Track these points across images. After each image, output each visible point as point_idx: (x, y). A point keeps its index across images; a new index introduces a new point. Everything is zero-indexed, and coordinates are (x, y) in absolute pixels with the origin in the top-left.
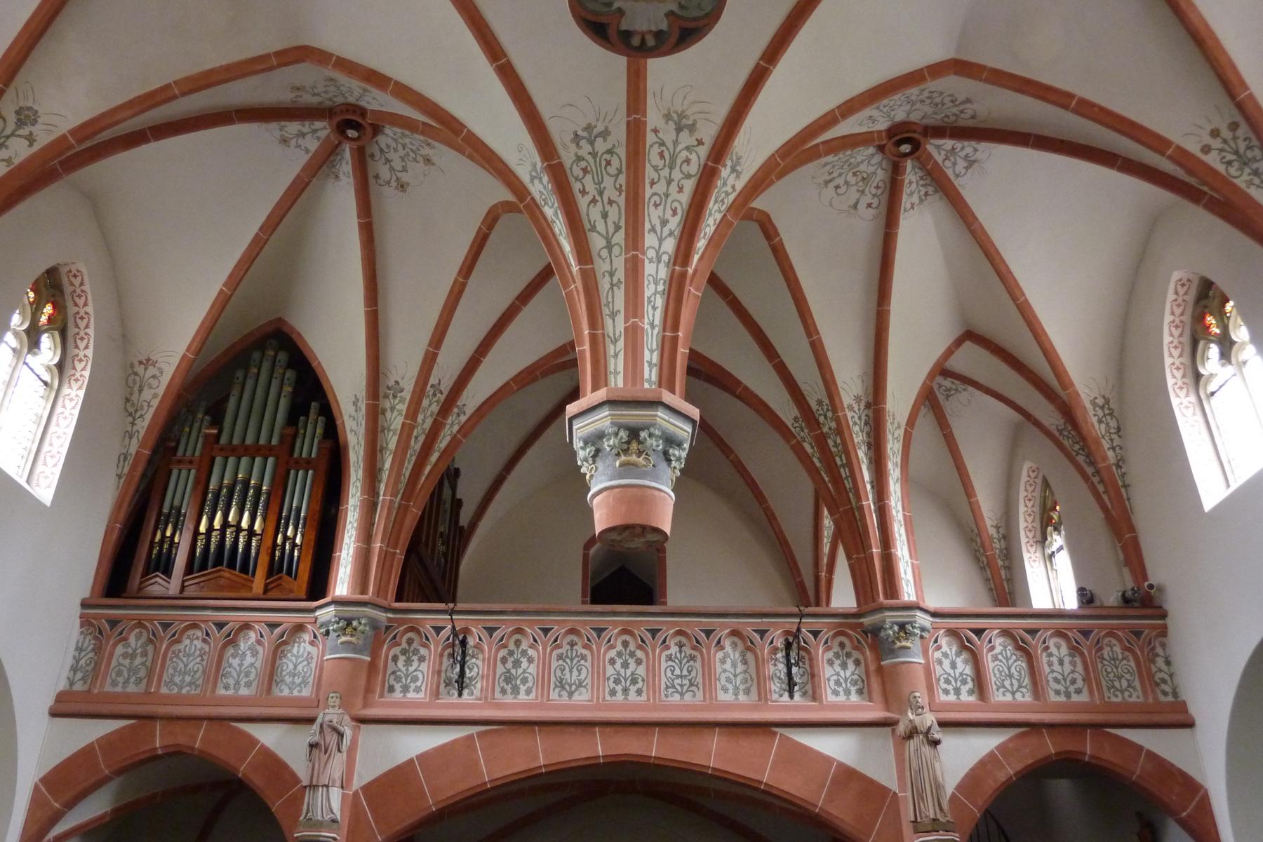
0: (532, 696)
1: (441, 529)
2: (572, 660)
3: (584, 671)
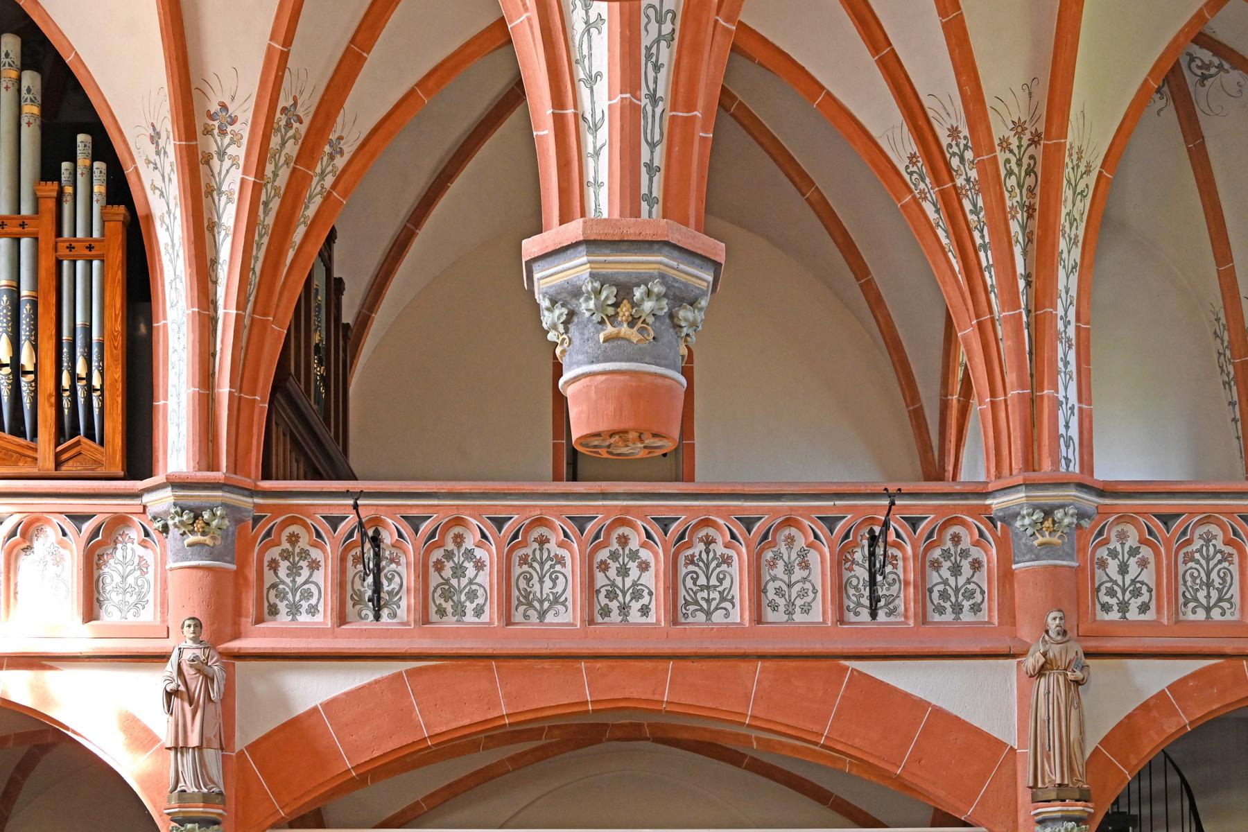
0: (485, 618)
1: (316, 338)
2: (542, 564)
3: (561, 580)
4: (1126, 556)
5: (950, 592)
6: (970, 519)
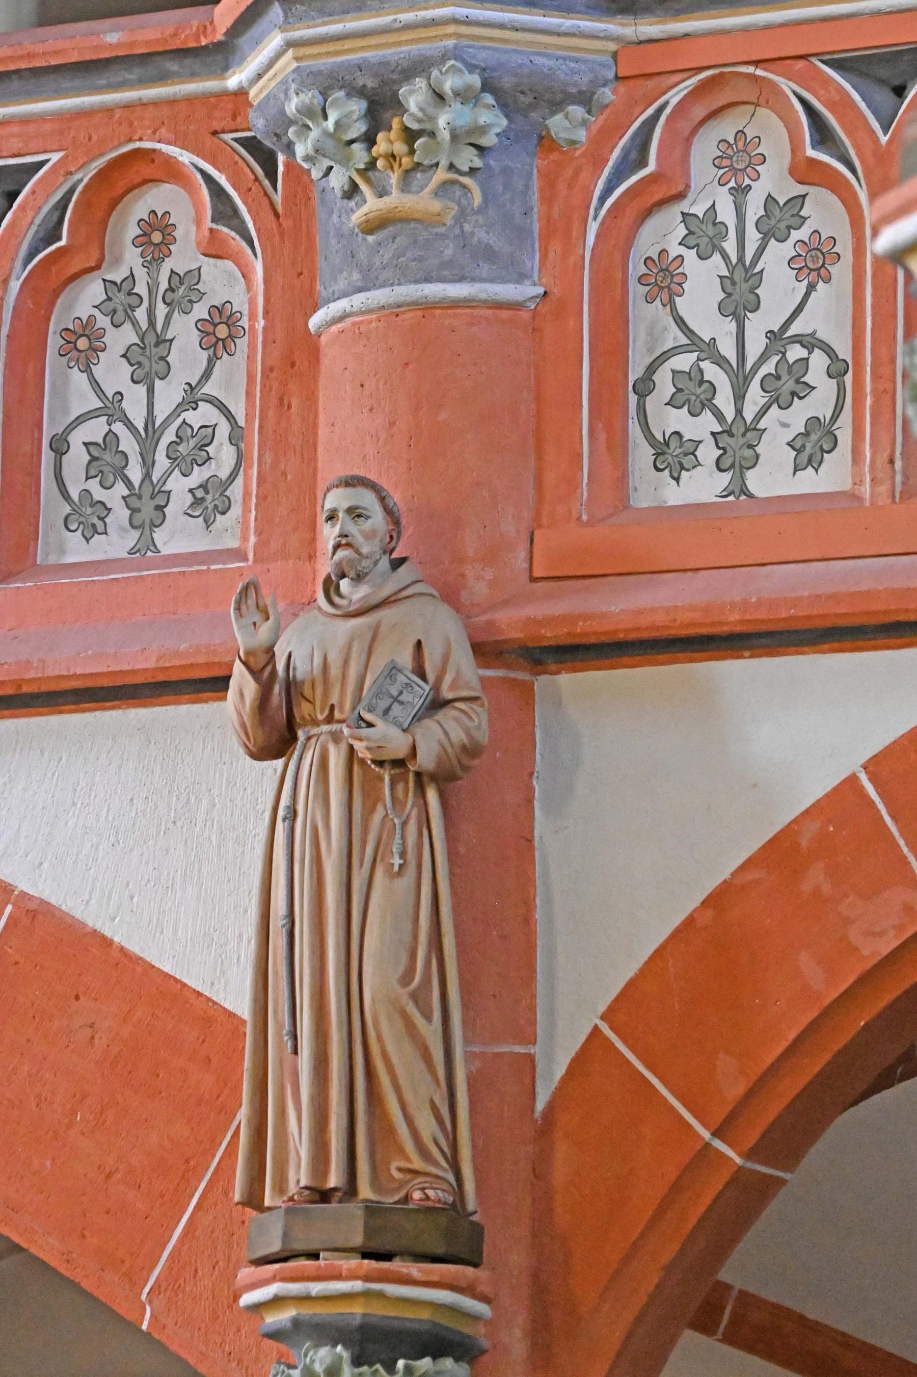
4: (753, 237)
5: (128, 444)
6: (185, 157)
